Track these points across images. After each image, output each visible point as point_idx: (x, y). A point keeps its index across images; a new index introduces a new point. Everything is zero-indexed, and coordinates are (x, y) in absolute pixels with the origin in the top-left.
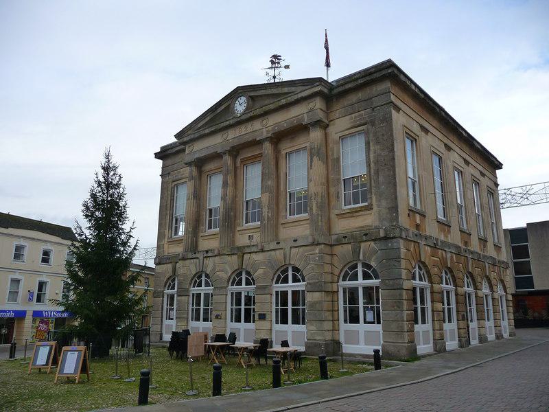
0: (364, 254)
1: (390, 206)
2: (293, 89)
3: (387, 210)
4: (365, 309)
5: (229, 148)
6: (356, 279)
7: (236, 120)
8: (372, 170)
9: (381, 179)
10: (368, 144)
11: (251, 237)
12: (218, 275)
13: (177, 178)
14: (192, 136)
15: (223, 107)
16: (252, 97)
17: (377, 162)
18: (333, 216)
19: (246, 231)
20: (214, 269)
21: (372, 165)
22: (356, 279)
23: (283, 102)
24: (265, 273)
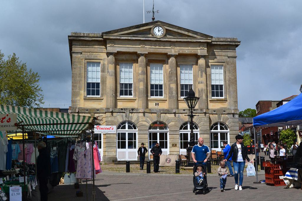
0: (223, 120)
1: (234, 100)
2: (195, 36)
3: (233, 102)
4: (221, 142)
5: (147, 53)
6: (217, 129)
7: (156, 39)
8: (227, 84)
9: (231, 88)
10: (225, 72)
11: (156, 104)
12: (141, 123)
13: (90, 57)
14: (119, 38)
15: (145, 28)
16: (166, 29)
17: (229, 81)
18: (209, 101)
19: (156, 101)
20: (138, 119)
21: (227, 82)
22: (217, 129)
23: (189, 40)
24: (175, 125)
